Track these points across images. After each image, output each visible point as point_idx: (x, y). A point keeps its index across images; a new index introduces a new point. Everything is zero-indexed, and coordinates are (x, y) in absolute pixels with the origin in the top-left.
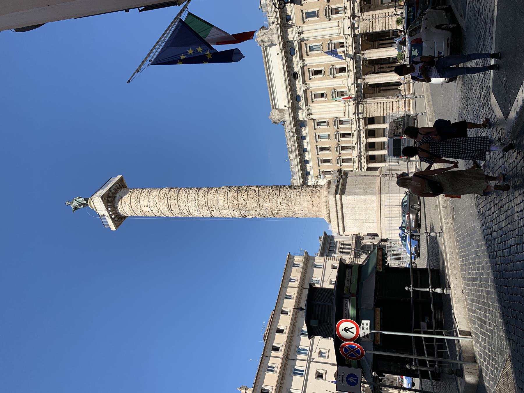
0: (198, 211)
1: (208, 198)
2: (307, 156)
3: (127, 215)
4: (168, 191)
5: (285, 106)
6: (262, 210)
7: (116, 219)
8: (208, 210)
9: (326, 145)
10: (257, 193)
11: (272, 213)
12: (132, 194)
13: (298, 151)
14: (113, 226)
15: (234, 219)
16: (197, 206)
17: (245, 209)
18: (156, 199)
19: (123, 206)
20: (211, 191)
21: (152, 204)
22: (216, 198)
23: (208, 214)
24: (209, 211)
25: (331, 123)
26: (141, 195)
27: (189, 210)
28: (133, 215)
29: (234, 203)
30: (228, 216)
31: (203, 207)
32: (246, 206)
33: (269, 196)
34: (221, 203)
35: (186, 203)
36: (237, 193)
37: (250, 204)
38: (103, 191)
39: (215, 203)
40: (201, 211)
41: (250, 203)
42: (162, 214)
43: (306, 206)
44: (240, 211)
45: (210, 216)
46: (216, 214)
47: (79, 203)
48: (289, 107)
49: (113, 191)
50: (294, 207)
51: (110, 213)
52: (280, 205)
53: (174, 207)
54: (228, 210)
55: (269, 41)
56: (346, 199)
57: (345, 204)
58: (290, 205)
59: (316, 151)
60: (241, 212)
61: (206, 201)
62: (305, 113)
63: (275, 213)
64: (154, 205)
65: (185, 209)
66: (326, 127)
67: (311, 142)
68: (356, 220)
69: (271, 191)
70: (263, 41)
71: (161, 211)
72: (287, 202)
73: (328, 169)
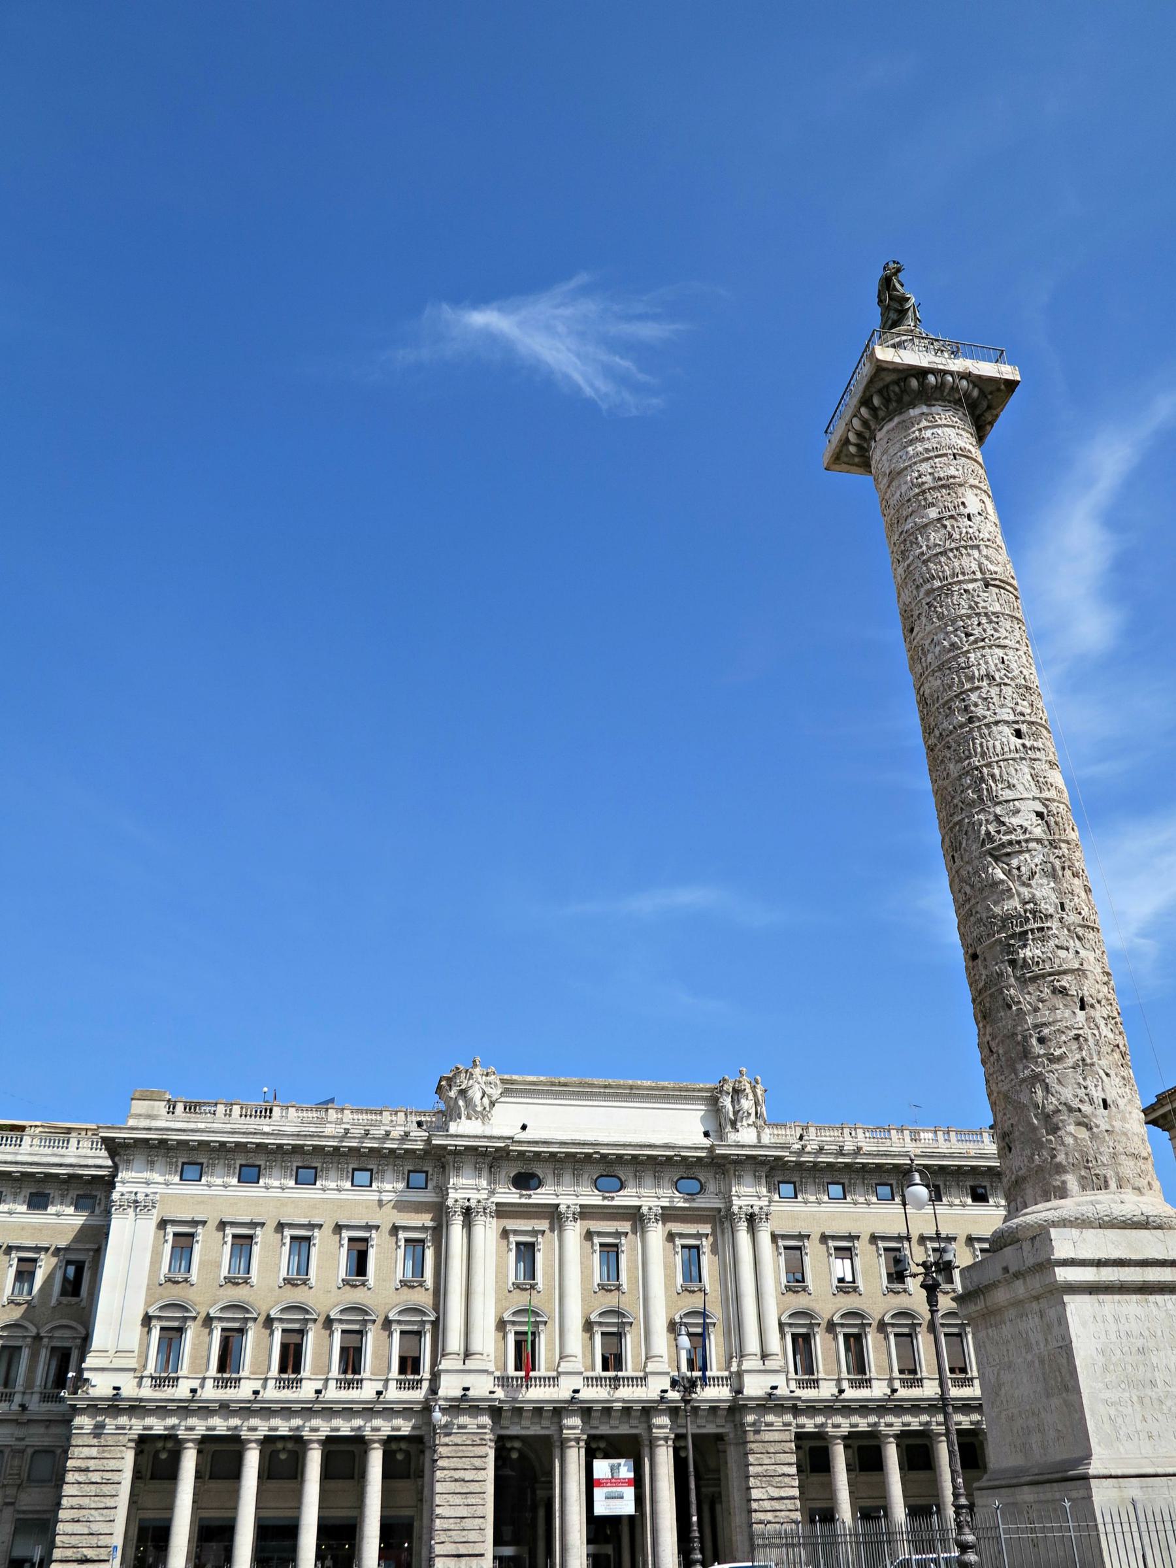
0: (1006, 681)
5: (524, 1127)
6: (1069, 930)
8: (1022, 718)
9: (319, 1267)
11: (1065, 972)
14: (897, 360)
24: (1012, 718)
43: (1127, 1126)
44: (1046, 843)
51: (950, 378)
55: (736, 1113)
59: (297, 1221)
60: (1039, 841)
66: (400, 1276)
68: (1142, 1351)
70: (737, 1093)
73: (200, 1263)
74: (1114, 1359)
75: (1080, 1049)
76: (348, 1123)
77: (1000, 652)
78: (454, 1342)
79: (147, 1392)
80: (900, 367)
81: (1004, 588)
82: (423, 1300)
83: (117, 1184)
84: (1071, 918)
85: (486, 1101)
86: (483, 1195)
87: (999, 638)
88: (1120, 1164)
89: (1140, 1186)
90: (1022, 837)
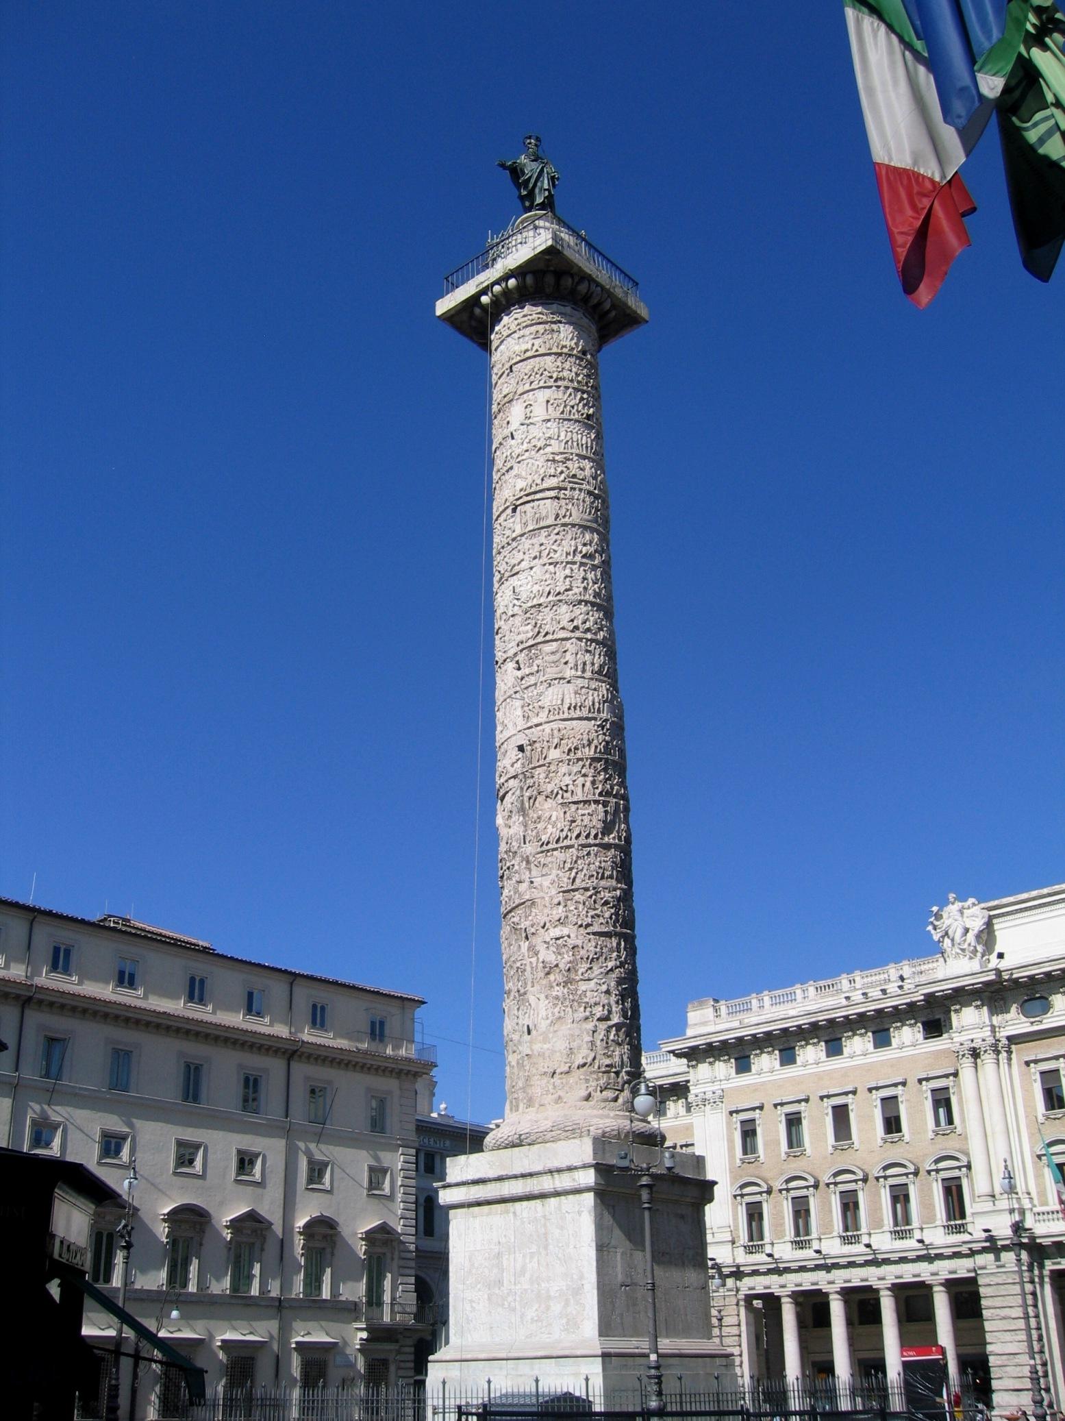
1: (568, 644)
2: (811, 1054)
3: (493, 349)
4: (592, 489)
5: (1001, 956)
6: (528, 862)
7: (477, 311)
10: (597, 842)
12: (573, 360)
13: (828, 1020)
15: (490, 753)
16: (535, 602)
17: (527, 794)
18: (556, 447)
19: (527, 331)
20: (597, 652)
21: (535, 431)
22: (569, 673)
23: (504, 646)
25: (949, 1145)
26: (570, 390)
27: (517, 573)
28: (495, 370)
29: (552, 750)
30: (499, 728)
31: (530, 627)
32: (540, 799)
33: (586, 889)
34: (551, 696)
35: (544, 560)
36: (594, 760)
37: (547, 815)
38: (578, 255)
39: (548, 670)
40: (518, 620)
41: (554, 814)
42: (499, 474)
43: (546, 1046)
44: (521, 777)
45: (499, 656)
46: (506, 679)
47: (533, 181)
48: (998, 972)
49: (583, 288)
50: (542, 996)
52: (548, 940)
53: (528, 514)
54: (521, 724)
56: (580, 1213)
57: (559, 1208)
58: (552, 977)
60: (514, 777)
61: (555, 636)
62: (981, 1036)
63: (516, 920)
64: (534, 442)
65: (521, 556)
67: (868, 1068)
69: (607, 895)
71: (511, 468)
72: (561, 966)
73: (765, 1144)
74: (476, 1265)
75: (518, 980)
76: (848, 992)
77: (514, 581)
78: (982, 1186)
79: (742, 1258)
80: (459, 307)
81: (533, 501)
82: (958, 1146)
83: (691, 1088)
84: (529, 849)
85: (971, 937)
86: (987, 1033)
87: (514, 566)
88: (531, 1086)
89: (546, 1102)
90: (506, 778)
